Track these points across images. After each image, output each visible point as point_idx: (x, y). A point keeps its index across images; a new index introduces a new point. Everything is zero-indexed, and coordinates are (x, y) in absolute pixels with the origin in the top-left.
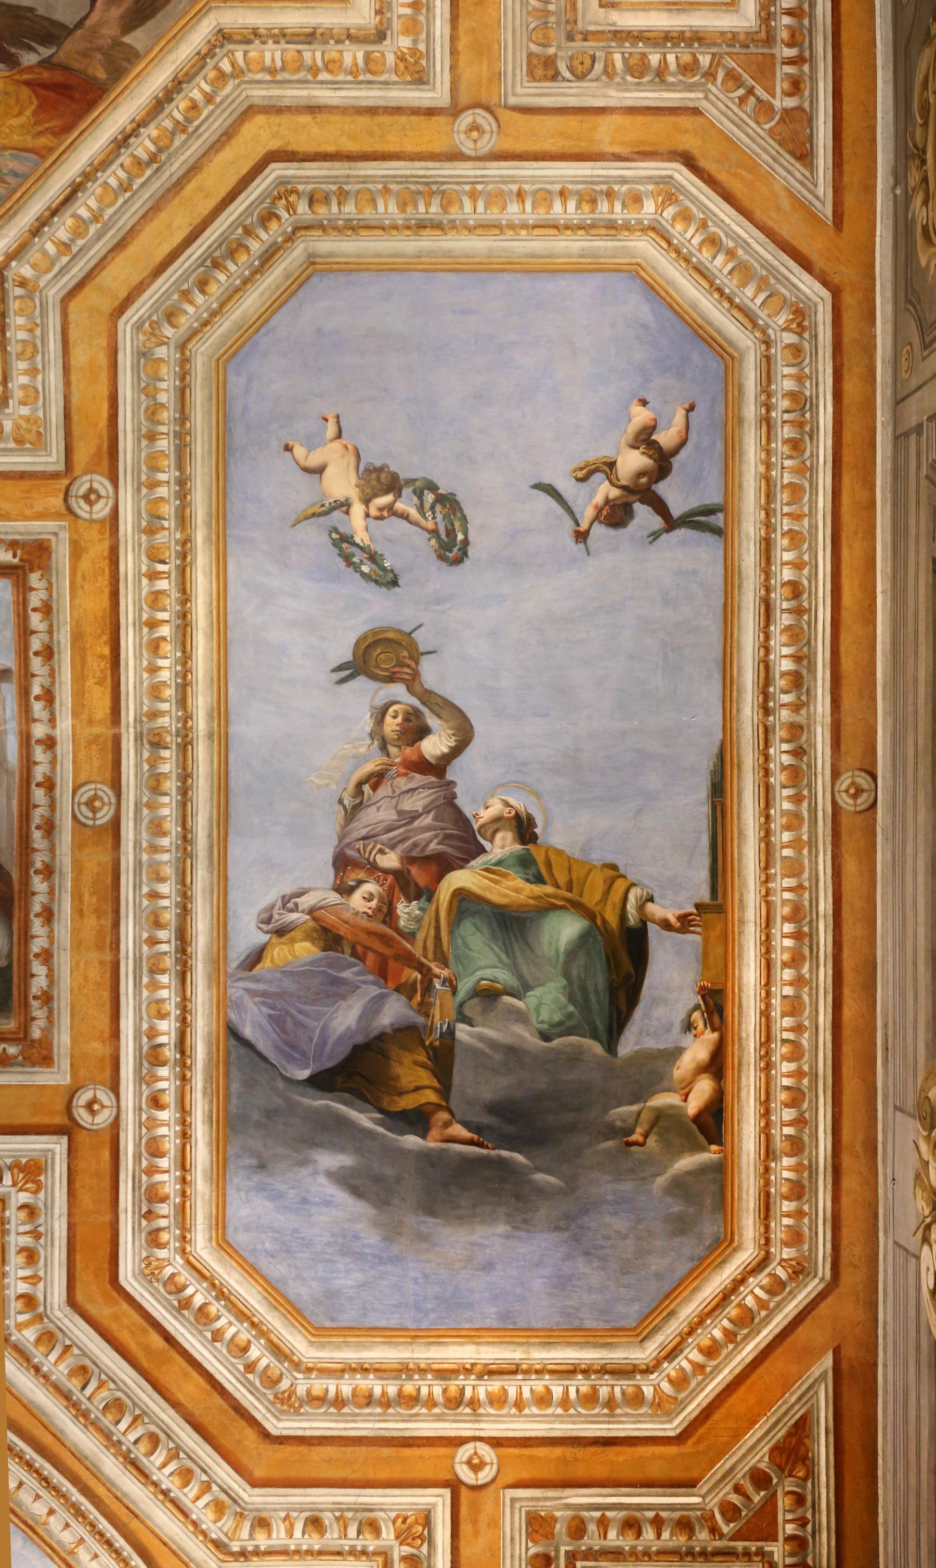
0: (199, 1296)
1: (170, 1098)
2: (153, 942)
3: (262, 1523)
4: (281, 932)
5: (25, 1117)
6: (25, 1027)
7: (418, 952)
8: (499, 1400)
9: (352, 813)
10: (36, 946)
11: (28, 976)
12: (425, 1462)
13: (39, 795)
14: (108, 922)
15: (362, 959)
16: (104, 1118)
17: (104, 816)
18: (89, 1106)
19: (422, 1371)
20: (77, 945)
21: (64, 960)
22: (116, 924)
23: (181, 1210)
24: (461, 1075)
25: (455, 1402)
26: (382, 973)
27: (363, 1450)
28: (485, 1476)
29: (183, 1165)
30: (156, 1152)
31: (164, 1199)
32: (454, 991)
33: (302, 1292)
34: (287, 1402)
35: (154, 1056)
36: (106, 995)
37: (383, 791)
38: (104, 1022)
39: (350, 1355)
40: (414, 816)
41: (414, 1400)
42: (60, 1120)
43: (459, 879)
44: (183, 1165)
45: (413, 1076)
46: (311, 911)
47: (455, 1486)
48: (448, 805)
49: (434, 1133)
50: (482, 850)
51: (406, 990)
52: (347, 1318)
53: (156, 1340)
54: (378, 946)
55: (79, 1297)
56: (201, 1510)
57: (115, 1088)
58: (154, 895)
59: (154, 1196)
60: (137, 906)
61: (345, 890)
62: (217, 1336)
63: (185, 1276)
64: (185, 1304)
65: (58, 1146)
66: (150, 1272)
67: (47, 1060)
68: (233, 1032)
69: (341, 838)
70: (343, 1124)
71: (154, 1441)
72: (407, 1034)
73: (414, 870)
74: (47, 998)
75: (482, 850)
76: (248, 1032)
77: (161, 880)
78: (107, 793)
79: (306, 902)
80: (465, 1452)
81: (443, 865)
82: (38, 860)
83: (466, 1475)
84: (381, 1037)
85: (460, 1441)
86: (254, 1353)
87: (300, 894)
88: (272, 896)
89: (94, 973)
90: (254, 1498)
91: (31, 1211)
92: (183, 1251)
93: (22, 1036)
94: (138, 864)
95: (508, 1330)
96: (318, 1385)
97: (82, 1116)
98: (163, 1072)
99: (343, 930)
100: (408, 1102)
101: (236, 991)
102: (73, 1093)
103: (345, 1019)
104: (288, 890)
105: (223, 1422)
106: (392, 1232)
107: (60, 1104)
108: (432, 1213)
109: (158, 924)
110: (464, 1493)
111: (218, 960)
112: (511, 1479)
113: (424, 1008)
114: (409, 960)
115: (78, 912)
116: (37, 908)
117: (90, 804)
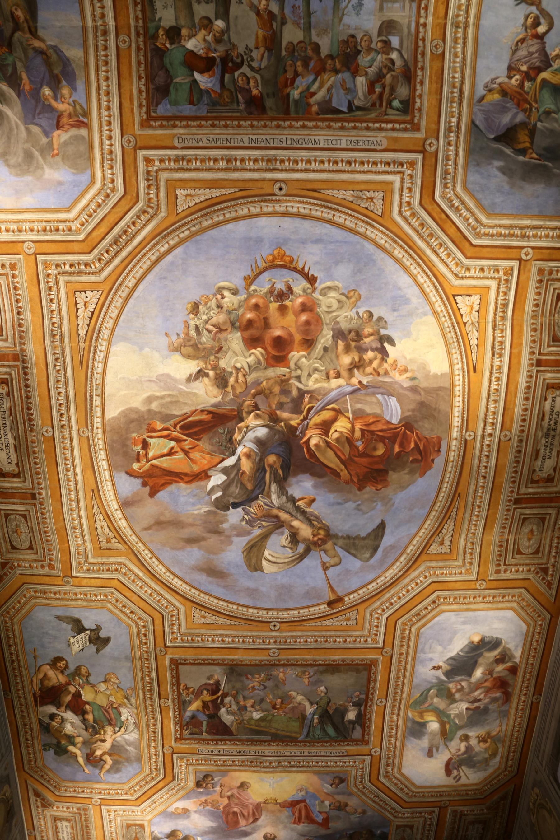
0: (456, 203)
1: (453, 143)
2: (452, 92)
3: (468, 269)
4: (490, 91)
5: (411, 147)
6: (413, 119)
7: (529, 98)
8: (535, 236)
9: (514, 52)
10: (418, 93)
11: (415, 102)
12: (513, 253)
13: (420, 43)
14: (439, 86)
15: (513, 100)
16: (433, 149)
17: (440, 51)
18: (430, 145)
19: (516, 227)
20: (430, 93)
21: (426, 98)
22: (442, 87)
23: (454, 177)
24: (538, 138)
25: (523, 236)
26: (518, 105)
27: (497, 250)
28: (529, 257)
29: (456, 163)
30: (448, 159)
31: (449, 174)
32: (538, 111)
33: (485, 202)
34: (478, 235)
35: (449, 130)
36: (437, 109)
37: (525, 45)
38: (436, 119)
39: (497, 222)
40: (532, 54)
41: (512, 235)
42: (421, 148)
43: (544, 75)
44: (456, 163)
45: (523, 137)
46: (500, 84)
47: (520, 260)
48: (543, 51)
49: (528, 156)
50: (551, 66)
51: (524, 111)
52: (497, 211)
53: (443, 216)
54: (518, 96)
55: (423, 203)
56: (452, 265)
57: (438, 139)
58: (454, 77)
59: (446, 173)
60: (448, 80)
61: (510, 78)
62: (461, 215)
63: (453, 197)
64: (453, 206)
65: (420, 157)
66: (443, 196)
67: (418, 130)
68: (473, 123)
69: (511, 60)
70: (502, 152)
71: (441, 245)
72: (523, 125)
73: (531, 72)
74: (420, 110)
75: (551, 66)
76: (477, 123)
77: (456, 72)
78: (441, 43)
79: (498, 81)
80: (524, 251)
81: (539, 70)
82: (420, 65)
83: (524, 257)
84: (516, 126)
85: (522, 248)
86: (470, 220)
87: (497, 78)
88: (488, 79)
89: (434, 102)
90: (467, 262)
91: (411, 176)
92: (453, 190)
93: (411, 122)
94: (449, 67)
95: (541, 215)
96: (487, 230)
97: (428, 148)
98: (452, 134)
99: (508, 91)
100: (521, 146)
101: (476, 109)
102: (425, 140)
103: (506, 120)
104: (493, 76)
105: (460, 240)
106: (512, 185)
107: (421, 144)
108: (524, 180)
109: (454, 87)
110: (523, 262)
111: (471, 99)
112: (535, 258)
113: (529, 117)
114: (526, 101)
115: (431, 82)
116: (418, 80)
117: (436, 46)
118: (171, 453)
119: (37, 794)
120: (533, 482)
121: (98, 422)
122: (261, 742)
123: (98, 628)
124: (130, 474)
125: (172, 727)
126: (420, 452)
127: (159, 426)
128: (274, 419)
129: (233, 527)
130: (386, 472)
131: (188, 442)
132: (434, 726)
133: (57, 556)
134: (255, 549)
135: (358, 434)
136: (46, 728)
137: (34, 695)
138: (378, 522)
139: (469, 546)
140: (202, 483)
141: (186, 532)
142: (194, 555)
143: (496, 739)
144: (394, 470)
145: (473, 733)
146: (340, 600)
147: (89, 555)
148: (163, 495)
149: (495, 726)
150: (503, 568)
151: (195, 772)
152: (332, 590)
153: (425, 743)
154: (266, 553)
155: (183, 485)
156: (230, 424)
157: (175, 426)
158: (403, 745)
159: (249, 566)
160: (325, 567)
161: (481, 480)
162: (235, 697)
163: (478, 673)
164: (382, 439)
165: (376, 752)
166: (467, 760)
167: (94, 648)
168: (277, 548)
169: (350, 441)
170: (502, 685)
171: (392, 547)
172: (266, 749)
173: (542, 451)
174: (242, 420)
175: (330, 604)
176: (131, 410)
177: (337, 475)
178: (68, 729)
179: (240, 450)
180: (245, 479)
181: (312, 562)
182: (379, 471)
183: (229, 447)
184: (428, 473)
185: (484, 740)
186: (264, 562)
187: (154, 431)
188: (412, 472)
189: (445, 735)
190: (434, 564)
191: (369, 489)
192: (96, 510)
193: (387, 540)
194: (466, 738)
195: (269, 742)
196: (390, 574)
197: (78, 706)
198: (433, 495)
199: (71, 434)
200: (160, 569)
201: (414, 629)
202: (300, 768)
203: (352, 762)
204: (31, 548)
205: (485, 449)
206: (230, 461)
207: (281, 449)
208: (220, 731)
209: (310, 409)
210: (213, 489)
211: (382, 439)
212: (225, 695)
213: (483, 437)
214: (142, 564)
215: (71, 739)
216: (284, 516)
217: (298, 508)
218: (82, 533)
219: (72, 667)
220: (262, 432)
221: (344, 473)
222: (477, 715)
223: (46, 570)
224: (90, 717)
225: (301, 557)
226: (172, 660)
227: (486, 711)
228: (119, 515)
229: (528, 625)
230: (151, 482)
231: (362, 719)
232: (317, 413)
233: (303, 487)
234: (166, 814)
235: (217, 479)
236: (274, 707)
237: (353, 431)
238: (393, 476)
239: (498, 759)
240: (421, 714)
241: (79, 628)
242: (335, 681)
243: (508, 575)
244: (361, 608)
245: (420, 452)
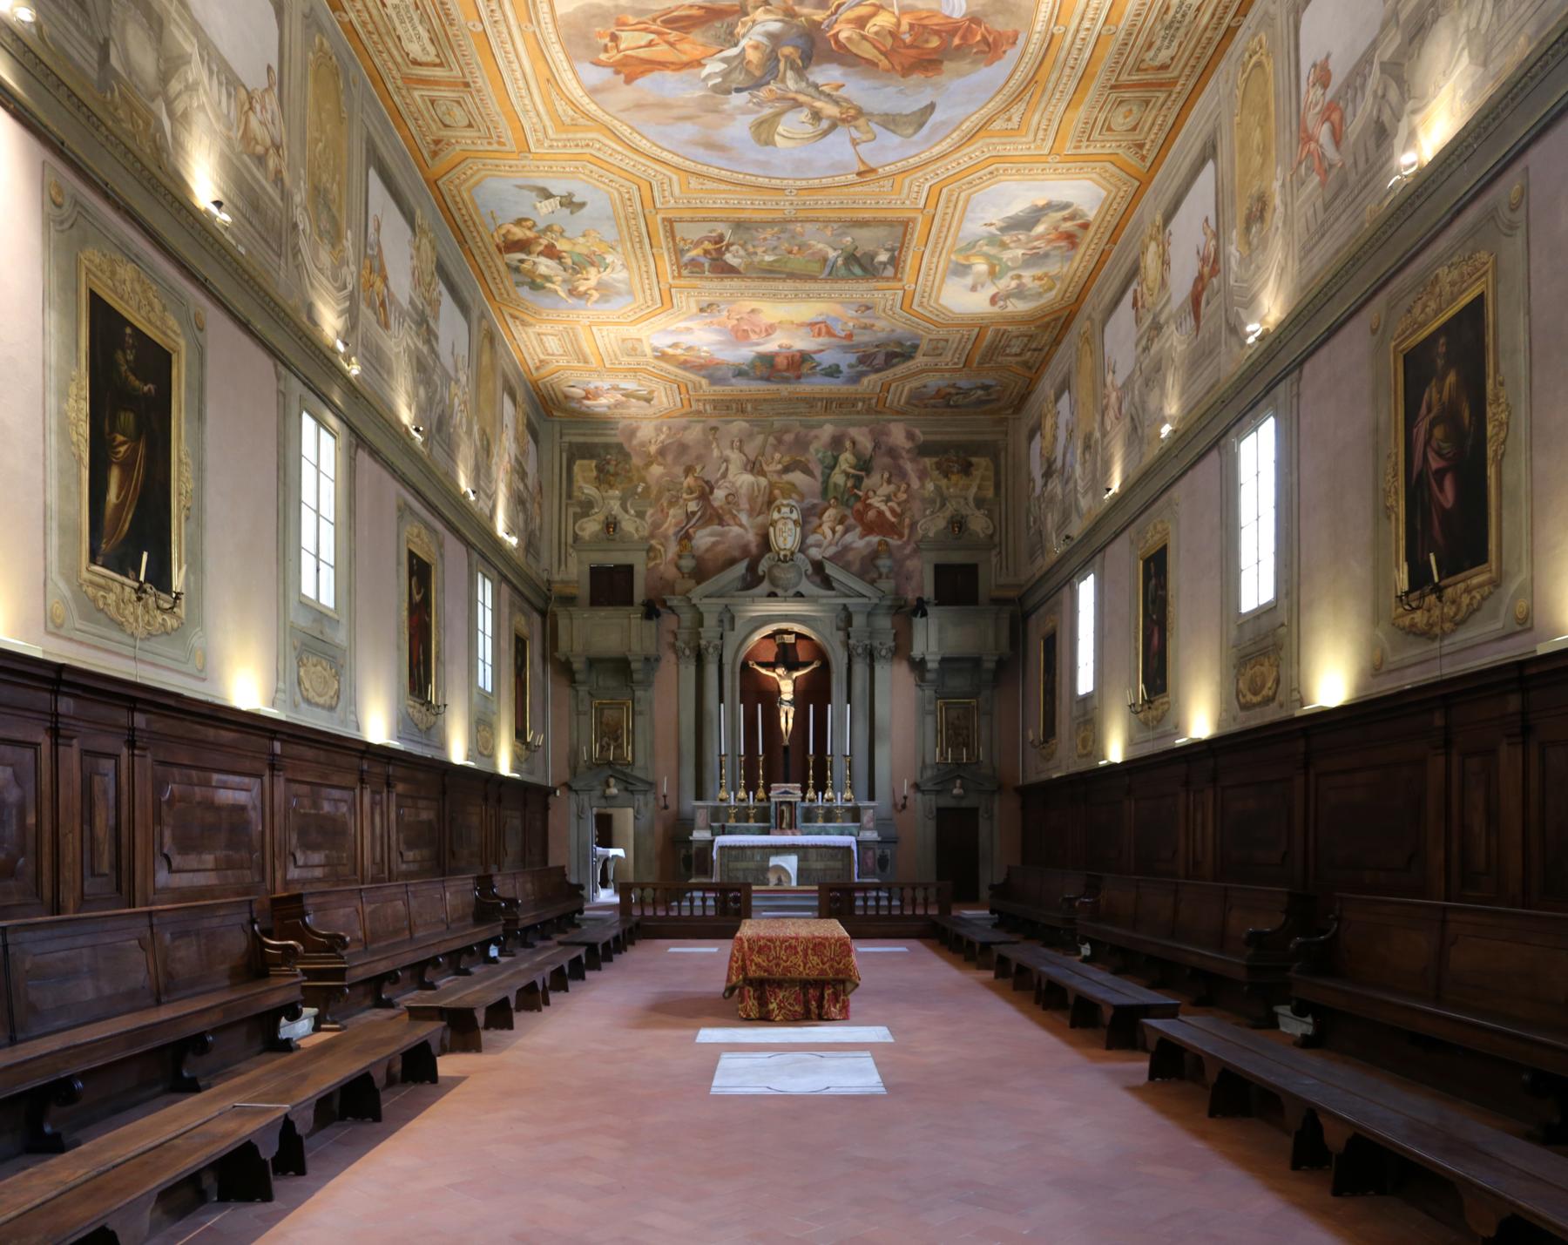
118: (650, 44)
119: (514, 317)
120: (1138, 70)
121: (545, 17)
122: (774, 279)
123: (570, 195)
124: (597, 63)
125: (667, 267)
126: (988, 45)
127: (632, 20)
128: (790, 14)
129: (737, 108)
130: (941, 62)
131: (673, 36)
132: (981, 267)
133: (508, 134)
134: (765, 125)
135: (905, 27)
136: (517, 270)
137: (497, 246)
138: (924, 103)
139: (1044, 122)
140: (695, 71)
141: (675, 112)
142: (688, 130)
143: (1053, 279)
144: (951, 60)
145: (1027, 275)
146: (873, 171)
147: (550, 132)
148: (640, 82)
149: (1054, 268)
150: (1085, 143)
151: (698, 302)
152: (863, 162)
153: (969, 280)
154: (780, 129)
155: (668, 73)
156: (730, 19)
157: (654, 20)
158: (943, 281)
159: (758, 141)
160: (855, 143)
161: (1067, 71)
162: (743, 246)
163: (1040, 229)
164: (937, 33)
165: (910, 287)
166: (1020, 293)
167: (567, 211)
168: (794, 125)
169: (893, 34)
170: (1071, 238)
171: (943, 123)
172: (780, 285)
173: (1158, 43)
174: (747, 14)
175: (859, 174)
176: (591, 6)
177: (875, 65)
178: (542, 270)
179: (743, 43)
180: (752, 68)
181: (840, 138)
182: (932, 62)
183: (731, 39)
184: (996, 64)
185: (1040, 279)
186: (777, 138)
187: (625, 24)
188: (974, 62)
189: (993, 274)
190: (995, 140)
191: (916, 77)
192: (554, 94)
193: (937, 117)
194: (1019, 277)
195: (784, 280)
196: (936, 151)
197: (551, 252)
198: (1002, 82)
199: (508, 27)
200: (644, 145)
201: (963, 195)
202: (819, 297)
203: (883, 295)
204: (470, 125)
205: (1078, 41)
206: (731, 52)
207: (800, 42)
208: (723, 270)
209: (839, 6)
210: (709, 76)
211: (937, 33)
212: (728, 246)
213: (1077, 31)
214: (619, 139)
215: (548, 279)
216: (802, 98)
217: (822, 93)
218: (538, 115)
219: (541, 226)
220: (775, 27)
221: (884, 62)
222: (1034, 259)
223: (495, 147)
224: (568, 261)
225: (825, 133)
226: (664, 220)
227: (1046, 255)
228: (586, 100)
229: (1109, 192)
230: (626, 70)
231: (895, 261)
232: (850, 8)
233: (827, 75)
234: (665, 331)
235: (714, 67)
236: (790, 252)
237: (898, 24)
238: (947, 65)
239: (1054, 292)
240: (967, 258)
241: (546, 194)
242: (864, 234)
243: (1091, 150)
244: (899, 178)
245: (988, 45)
